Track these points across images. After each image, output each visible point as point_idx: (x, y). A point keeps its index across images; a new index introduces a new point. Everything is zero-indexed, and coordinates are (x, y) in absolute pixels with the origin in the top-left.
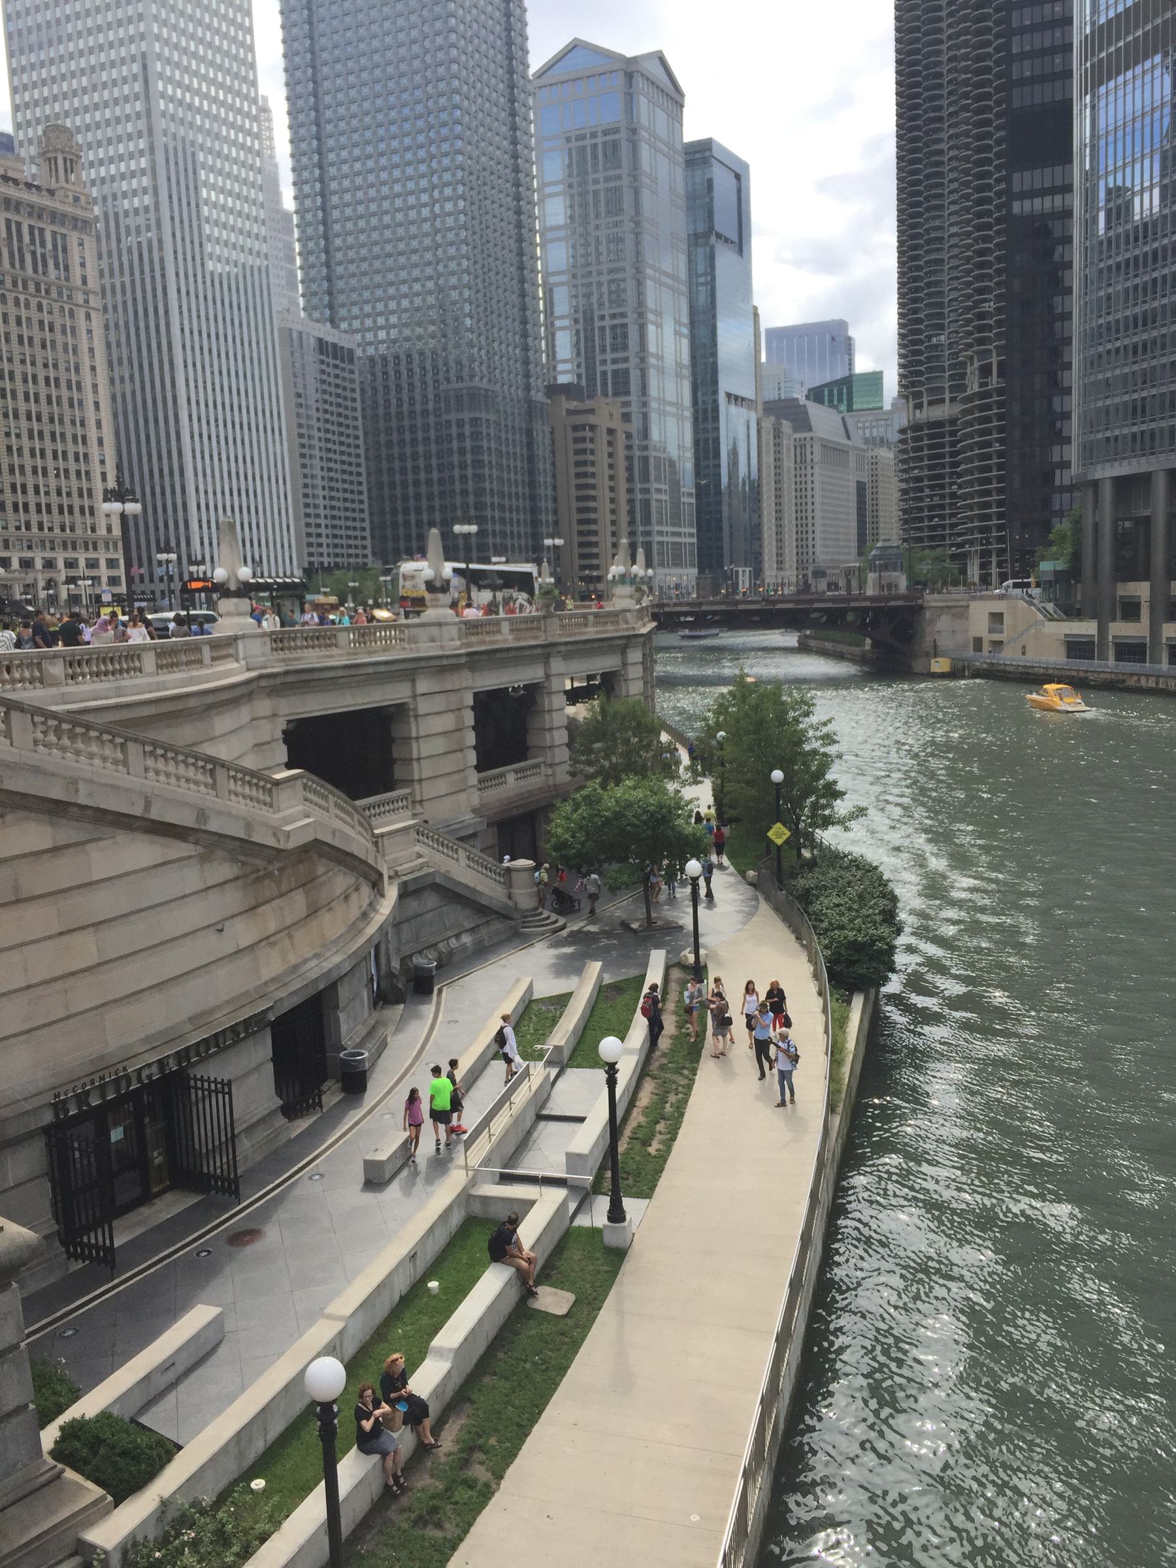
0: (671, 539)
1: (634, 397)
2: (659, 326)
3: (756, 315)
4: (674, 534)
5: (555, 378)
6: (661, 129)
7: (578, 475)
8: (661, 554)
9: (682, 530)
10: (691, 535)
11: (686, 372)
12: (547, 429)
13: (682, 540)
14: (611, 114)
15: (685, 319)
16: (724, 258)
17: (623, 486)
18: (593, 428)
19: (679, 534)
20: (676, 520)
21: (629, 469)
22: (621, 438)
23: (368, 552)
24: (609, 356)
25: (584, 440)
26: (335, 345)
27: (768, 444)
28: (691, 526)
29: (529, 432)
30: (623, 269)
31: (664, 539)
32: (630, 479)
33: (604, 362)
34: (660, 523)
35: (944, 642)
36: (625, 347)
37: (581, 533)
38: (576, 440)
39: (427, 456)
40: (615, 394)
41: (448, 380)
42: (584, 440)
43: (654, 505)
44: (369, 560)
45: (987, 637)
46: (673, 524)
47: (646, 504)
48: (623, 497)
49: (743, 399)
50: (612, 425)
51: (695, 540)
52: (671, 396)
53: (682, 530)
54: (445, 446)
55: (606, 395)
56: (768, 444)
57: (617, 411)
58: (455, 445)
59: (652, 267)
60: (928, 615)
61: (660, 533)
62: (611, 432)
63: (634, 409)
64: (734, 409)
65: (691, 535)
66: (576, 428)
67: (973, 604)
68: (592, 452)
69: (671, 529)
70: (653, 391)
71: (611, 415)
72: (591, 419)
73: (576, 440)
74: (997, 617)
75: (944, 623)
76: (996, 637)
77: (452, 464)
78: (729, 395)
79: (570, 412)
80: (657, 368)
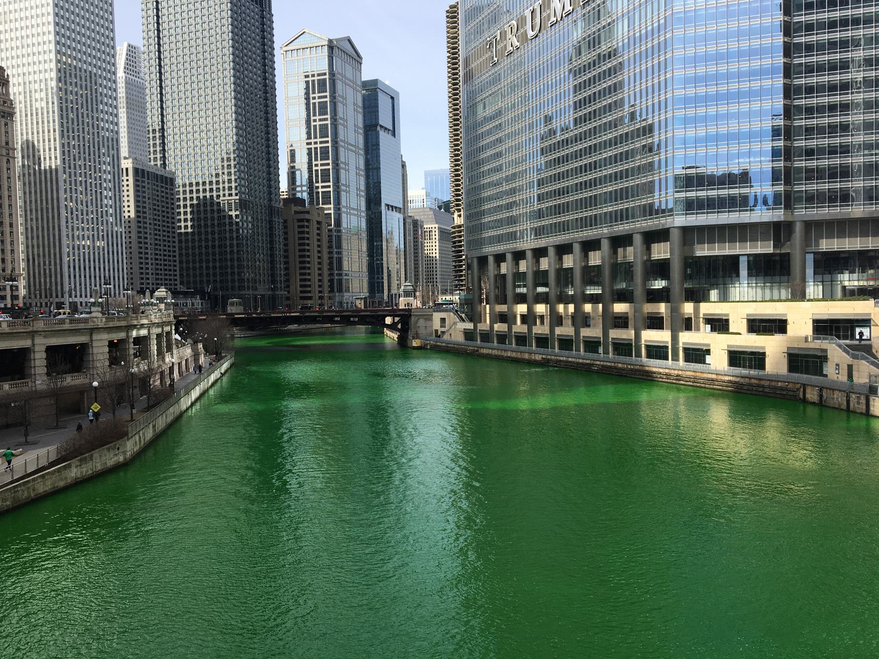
2: (347, 170)
3: (404, 166)
5: (295, 194)
6: (349, 73)
7: (300, 245)
11: (363, 194)
12: (281, 221)
15: (362, 166)
16: (384, 137)
17: (325, 250)
18: (308, 221)
21: (330, 241)
23: (178, 282)
25: (303, 226)
26: (162, 176)
27: (410, 230)
29: (271, 222)
32: (330, 247)
35: (422, 331)
37: (301, 274)
38: (299, 227)
39: (213, 233)
41: (224, 195)
42: (303, 226)
44: (178, 287)
45: (440, 330)
48: (325, 256)
49: (396, 208)
50: (319, 219)
52: (354, 205)
54: (223, 228)
56: (410, 230)
58: (227, 228)
59: (344, 141)
60: (413, 318)
62: (319, 223)
64: (390, 212)
66: (300, 220)
67: (434, 314)
68: (308, 233)
70: (343, 203)
72: (307, 216)
73: (299, 227)
74: (443, 320)
75: (421, 322)
76: (443, 329)
77: (225, 237)
78: (388, 205)
79: (296, 212)
80: (345, 191)
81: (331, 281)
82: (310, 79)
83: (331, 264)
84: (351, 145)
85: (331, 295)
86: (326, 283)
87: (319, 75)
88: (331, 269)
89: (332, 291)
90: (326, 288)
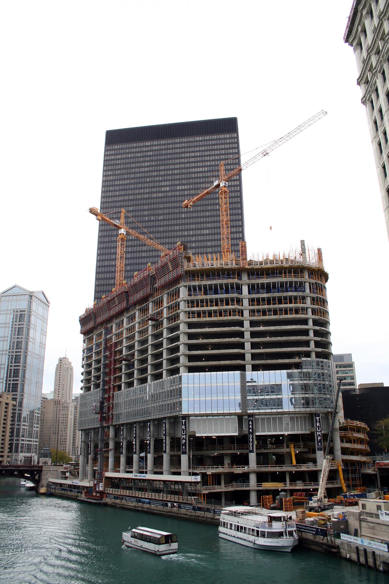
0: (27, 443)
1: (18, 393)
4: (28, 441)
8: (22, 448)
9: (33, 440)
10: (36, 441)
13: (32, 443)
14: (23, 305)
19: (31, 441)
20: (30, 435)
22: (10, 407)
24: (12, 379)
28: (37, 438)
30: (20, 352)
31: (24, 442)
33: (10, 380)
34: (23, 436)
36: (18, 376)
40: (12, 391)
43: (21, 430)
46: (28, 437)
47: (18, 430)
48: (9, 427)
51: (37, 444)
53: (33, 440)
55: (9, 391)
57: (10, 397)
61: (23, 440)
62: (7, 404)
63: (18, 397)
65: (36, 441)
69: (27, 439)
71: (8, 398)
81: (11, 445)
82: (15, 313)
83: (12, 432)
84: (36, 355)
85: (10, 454)
86: (7, 446)
87: (21, 311)
88: (12, 436)
89: (11, 451)
90: (7, 450)
